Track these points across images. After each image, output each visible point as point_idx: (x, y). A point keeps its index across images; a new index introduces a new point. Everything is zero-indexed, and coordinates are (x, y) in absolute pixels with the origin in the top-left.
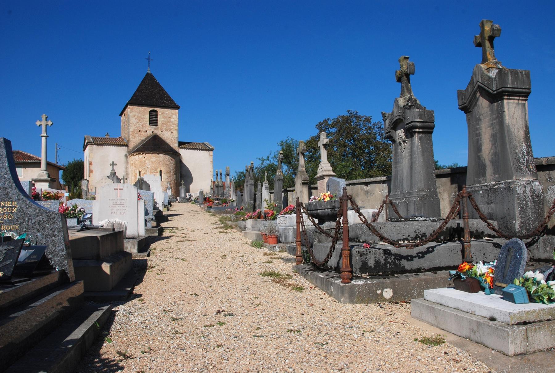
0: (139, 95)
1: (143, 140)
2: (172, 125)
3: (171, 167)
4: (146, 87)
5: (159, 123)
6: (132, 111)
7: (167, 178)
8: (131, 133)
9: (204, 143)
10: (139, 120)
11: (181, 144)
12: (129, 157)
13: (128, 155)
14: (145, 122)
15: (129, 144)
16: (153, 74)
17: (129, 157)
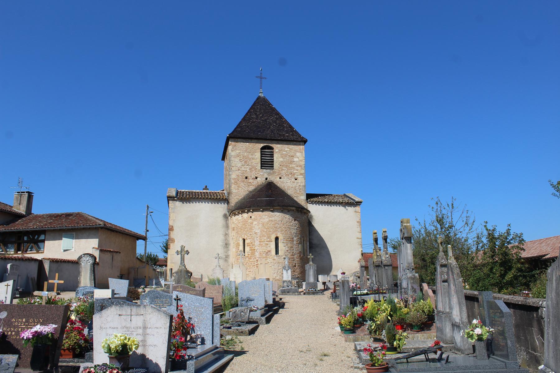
0: (245, 125)
2: (296, 168)
3: (294, 231)
4: (256, 114)
5: (276, 165)
7: (287, 249)
8: (233, 181)
9: (346, 194)
10: (246, 162)
11: (309, 196)
13: (228, 214)
14: (254, 164)
15: (230, 197)
16: (268, 98)
17: (229, 217)
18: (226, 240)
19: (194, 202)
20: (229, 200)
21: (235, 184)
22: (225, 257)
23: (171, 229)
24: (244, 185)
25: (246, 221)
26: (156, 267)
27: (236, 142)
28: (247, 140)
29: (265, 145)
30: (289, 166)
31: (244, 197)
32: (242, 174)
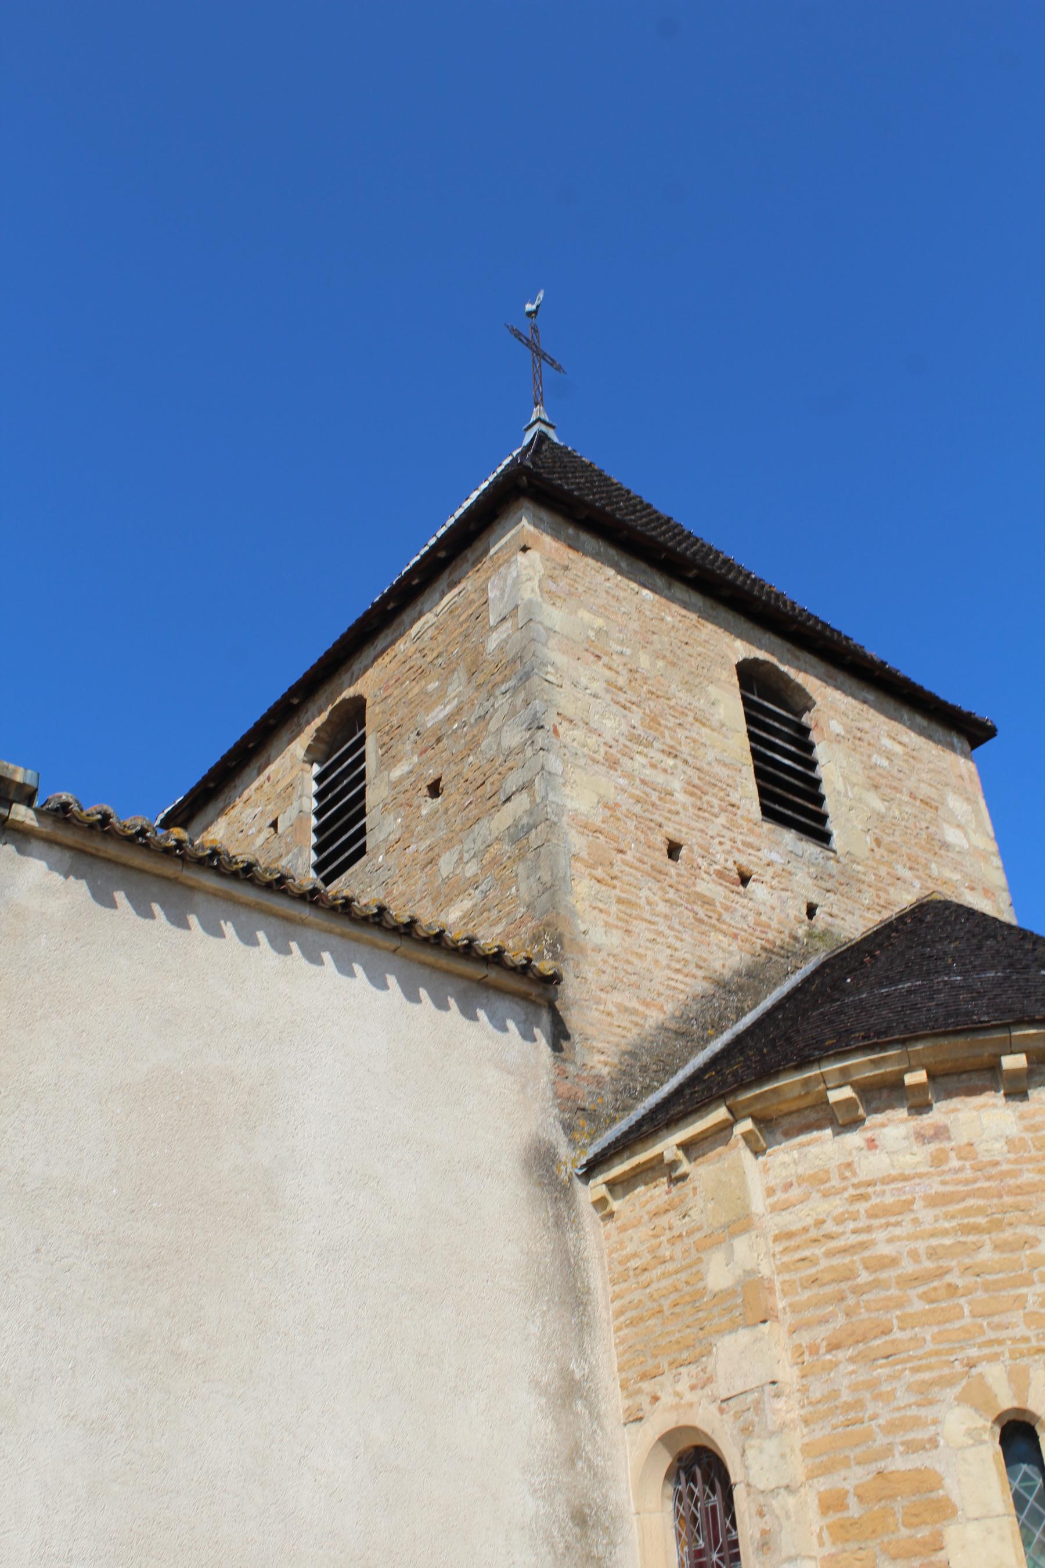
1: (721, 984)
6: (563, 583)
8: (577, 842)
10: (653, 721)
18: (571, 1462)
19: (228, 928)
20: (567, 1009)
21: (594, 872)
24: (662, 907)
25: (1020, 1191)
27: (570, 546)
28: (643, 566)
29: (762, 655)
30: (927, 867)
31: (684, 1018)
32: (637, 809)
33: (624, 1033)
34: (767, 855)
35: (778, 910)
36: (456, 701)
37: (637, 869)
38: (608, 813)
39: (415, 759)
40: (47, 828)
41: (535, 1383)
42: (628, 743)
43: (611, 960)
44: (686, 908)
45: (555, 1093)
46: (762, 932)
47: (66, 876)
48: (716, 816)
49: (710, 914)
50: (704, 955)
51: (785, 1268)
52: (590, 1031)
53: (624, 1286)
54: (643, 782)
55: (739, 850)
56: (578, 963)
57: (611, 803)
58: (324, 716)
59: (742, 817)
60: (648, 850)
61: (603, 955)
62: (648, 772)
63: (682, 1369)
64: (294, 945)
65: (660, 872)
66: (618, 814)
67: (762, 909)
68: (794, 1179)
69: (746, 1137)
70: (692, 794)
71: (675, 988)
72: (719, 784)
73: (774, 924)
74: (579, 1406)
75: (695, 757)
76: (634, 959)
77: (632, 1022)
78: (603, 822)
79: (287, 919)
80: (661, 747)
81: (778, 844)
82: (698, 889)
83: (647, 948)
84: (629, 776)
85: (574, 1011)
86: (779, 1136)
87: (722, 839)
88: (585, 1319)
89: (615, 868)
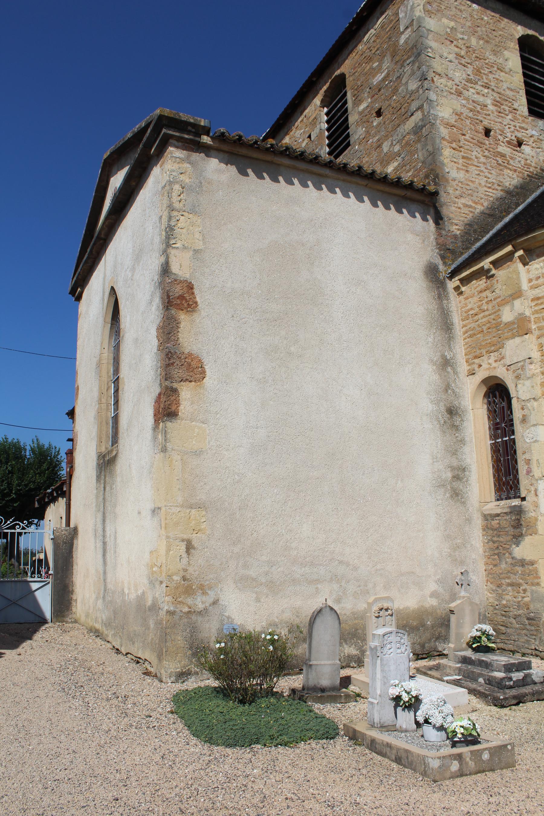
1: (508, 192)
8: (444, 132)
12: (451, 284)
18: (447, 391)
19: (296, 181)
20: (441, 207)
21: (452, 145)
22: (449, 475)
23: (182, 297)
24: (483, 159)
26: (13, 527)
31: (492, 208)
32: (471, 114)
33: (466, 216)
34: (531, 132)
35: (535, 158)
36: (386, 71)
37: (471, 142)
38: (457, 117)
39: (369, 100)
40: (217, 145)
41: (431, 361)
42: (466, 83)
43: (460, 184)
44: (493, 159)
45: (437, 243)
46: (527, 168)
47: (227, 165)
48: (507, 115)
49: (504, 161)
50: (501, 180)
51: (536, 312)
52: (451, 215)
53: (467, 322)
54: (473, 101)
55: (517, 131)
56: (446, 186)
57: (459, 113)
58: (328, 84)
59: (519, 115)
60: (476, 133)
61: (456, 182)
62: (475, 96)
63: (491, 354)
64: (324, 186)
65: (481, 143)
66: (462, 117)
67: (528, 157)
68: (541, 275)
69: (520, 257)
70: (496, 105)
71: (488, 195)
72: (509, 100)
73: (533, 164)
74: (449, 369)
75: (497, 87)
76: (470, 183)
77: (469, 211)
78: (455, 122)
79: (320, 175)
80: (482, 84)
81: (535, 127)
82: (499, 150)
83: (476, 178)
84: (467, 99)
85: (444, 207)
86: (534, 257)
87: (510, 126)
88: (451, 335)
89: (461, 143)
